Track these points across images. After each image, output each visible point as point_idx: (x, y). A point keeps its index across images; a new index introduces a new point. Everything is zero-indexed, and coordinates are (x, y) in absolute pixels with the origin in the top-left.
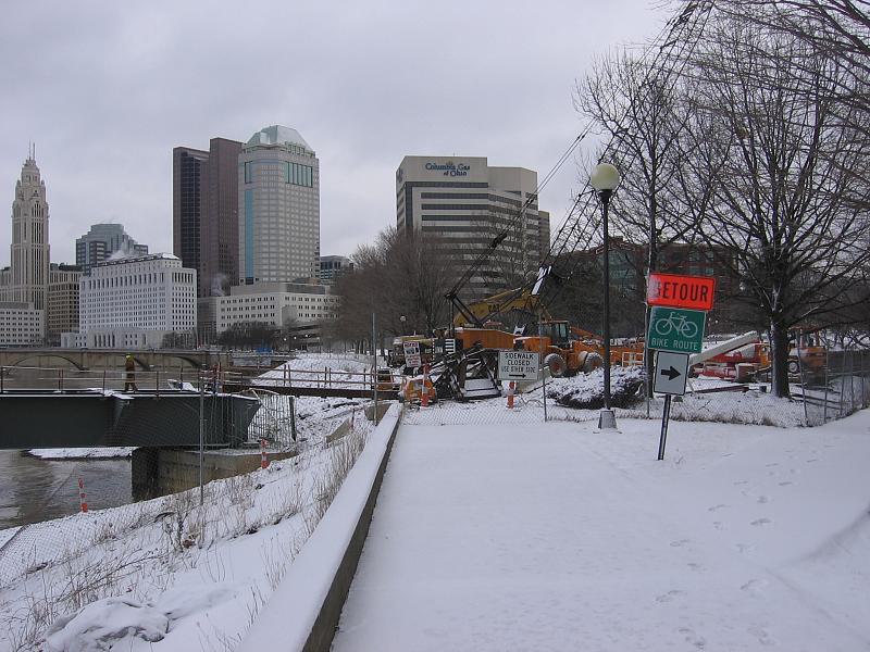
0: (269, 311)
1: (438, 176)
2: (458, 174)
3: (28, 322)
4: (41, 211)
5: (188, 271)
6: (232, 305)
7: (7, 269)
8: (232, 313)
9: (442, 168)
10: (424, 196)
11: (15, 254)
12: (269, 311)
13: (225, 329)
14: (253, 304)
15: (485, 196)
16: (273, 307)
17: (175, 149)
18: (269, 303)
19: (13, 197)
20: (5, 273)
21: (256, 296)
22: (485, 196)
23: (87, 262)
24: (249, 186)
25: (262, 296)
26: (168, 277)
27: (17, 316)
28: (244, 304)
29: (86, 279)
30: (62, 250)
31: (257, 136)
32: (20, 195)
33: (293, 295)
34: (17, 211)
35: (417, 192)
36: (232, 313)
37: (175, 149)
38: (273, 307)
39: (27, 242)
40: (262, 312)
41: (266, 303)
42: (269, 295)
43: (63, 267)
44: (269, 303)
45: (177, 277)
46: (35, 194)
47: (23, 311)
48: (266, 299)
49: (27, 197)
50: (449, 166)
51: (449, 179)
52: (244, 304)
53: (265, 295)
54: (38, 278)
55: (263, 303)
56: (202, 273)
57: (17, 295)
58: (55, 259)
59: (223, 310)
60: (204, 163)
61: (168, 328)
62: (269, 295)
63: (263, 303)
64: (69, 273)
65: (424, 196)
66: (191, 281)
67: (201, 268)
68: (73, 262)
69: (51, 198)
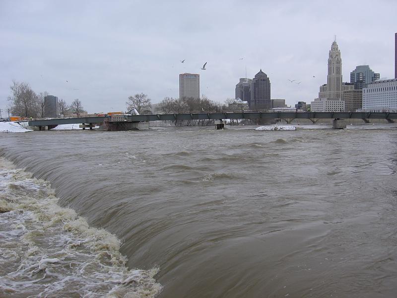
3: (338, 105)
4: (339, 62)
7: (325, 85)
11: (329, 79)
19: (328, 57)
20: (324, 86)
29: (366, 89)
30: (346, 78)
32: (331, 56)
34: (330, 63)
39: (334, 75)
43: (346, 84)
46: (337, 55)
47: (338, 101)
49: (334, 57)
54: (338, 89)
57: (330, 95)
58: (344, 81)
64: (349, 86)
68: (349, 82)
69: (342, 57)
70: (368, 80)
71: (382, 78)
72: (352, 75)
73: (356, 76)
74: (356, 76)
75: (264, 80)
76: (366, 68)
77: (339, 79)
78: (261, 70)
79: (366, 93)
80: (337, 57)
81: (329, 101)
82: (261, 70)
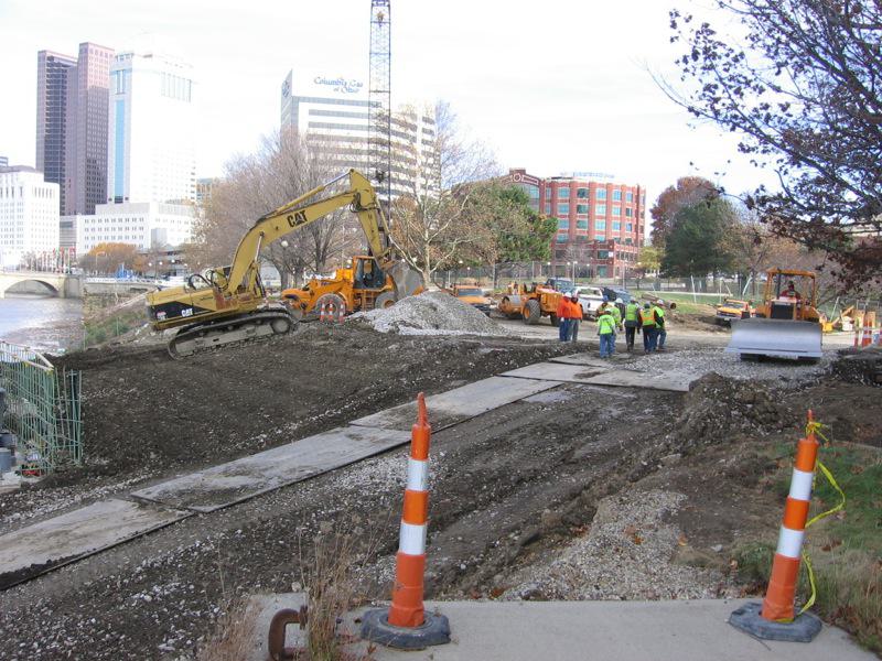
1: (327, 92)
2: (349, 90)
6: (97, 225)
8: (97, 233)
10: (312, 112)
13: (87, 251)
14: (120, 224)
17: (42, 55)
18: (138, 224)
21: (123, 216)
24: (121, 97)
25: (131, 216)
26: (28, 192)
35: (304, 108)
36: (97, 233)
37: (42, 55)
38: (142, 229)
40: (130, 233)
41: (134, 224)
42: (137, 216)
44: (138, 224)
45: (38, 192)
48: (127, 220)
55: (131, 224)
56: (67, 189)
59: (87, 230)
60: (73, 69)
61: (27, 248)
65: (312, 112)
67: (67, 183)
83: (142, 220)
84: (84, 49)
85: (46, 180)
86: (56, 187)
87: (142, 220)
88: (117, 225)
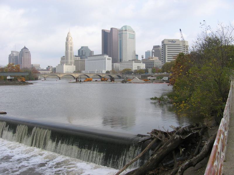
0: (131, 67)
1: (170, 43)
2: (174, 42)
5: (110, 58)
7: (64, 56)
9: (171, 41)
12: (131, 67)
15: (179, 46)
16: (132, 66)
20: (64, 57)
22: (179, 46)
23: (81, 55)
26: (107, 59)
27: (70, 67)
28: (125, 65)
29: (87, 59)
31: (122, 28)
33: (136, 63)
37: (102, 30)
38: (132, 66)
40: (130, 67)
42: (131, 63)
43: (76, 56)
44: (131, 65)
45: (108, 59)
48: (130, 64)
50: (173, 41)
51: (172, 43)
52: (125, 65)
53: (130, 63)
54: (71, 59)
60: (109, 33)
62: (131, 63)
63: (130, 65)
64: (77, 57)
66: (110, 60)
68: (77, 55)
70: (88, 55)
71: (95, 54)
72: (79, 51)
73: (81, 52)
74: (81, 52)
75: (27, 52)
76: (87, 48)
77: (71, 53)
78: (25, 47)
79: (87, 62)
80: (71, 41)
81: (67, 66)
82: (25, 47)
83: (132, 64)
84: (112, 29)
85: (109, 57)
86: (111, 58)
87: (132, 64)
88: (127, 65)
